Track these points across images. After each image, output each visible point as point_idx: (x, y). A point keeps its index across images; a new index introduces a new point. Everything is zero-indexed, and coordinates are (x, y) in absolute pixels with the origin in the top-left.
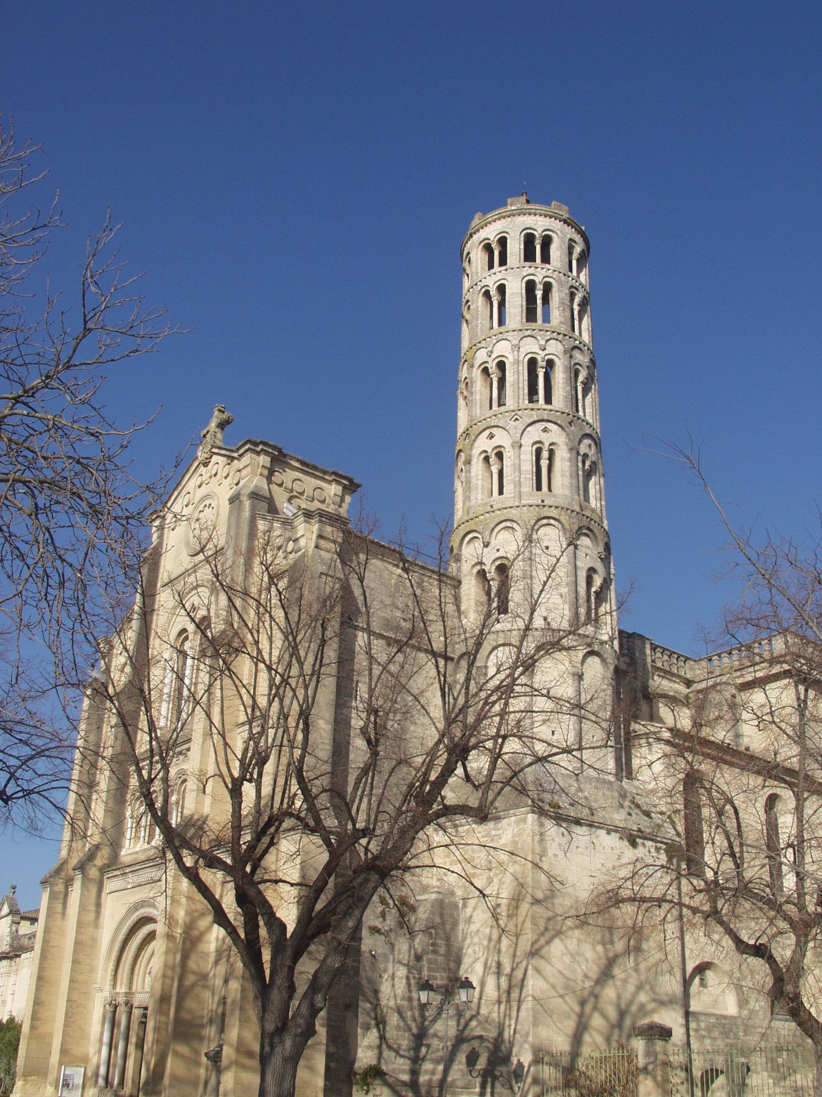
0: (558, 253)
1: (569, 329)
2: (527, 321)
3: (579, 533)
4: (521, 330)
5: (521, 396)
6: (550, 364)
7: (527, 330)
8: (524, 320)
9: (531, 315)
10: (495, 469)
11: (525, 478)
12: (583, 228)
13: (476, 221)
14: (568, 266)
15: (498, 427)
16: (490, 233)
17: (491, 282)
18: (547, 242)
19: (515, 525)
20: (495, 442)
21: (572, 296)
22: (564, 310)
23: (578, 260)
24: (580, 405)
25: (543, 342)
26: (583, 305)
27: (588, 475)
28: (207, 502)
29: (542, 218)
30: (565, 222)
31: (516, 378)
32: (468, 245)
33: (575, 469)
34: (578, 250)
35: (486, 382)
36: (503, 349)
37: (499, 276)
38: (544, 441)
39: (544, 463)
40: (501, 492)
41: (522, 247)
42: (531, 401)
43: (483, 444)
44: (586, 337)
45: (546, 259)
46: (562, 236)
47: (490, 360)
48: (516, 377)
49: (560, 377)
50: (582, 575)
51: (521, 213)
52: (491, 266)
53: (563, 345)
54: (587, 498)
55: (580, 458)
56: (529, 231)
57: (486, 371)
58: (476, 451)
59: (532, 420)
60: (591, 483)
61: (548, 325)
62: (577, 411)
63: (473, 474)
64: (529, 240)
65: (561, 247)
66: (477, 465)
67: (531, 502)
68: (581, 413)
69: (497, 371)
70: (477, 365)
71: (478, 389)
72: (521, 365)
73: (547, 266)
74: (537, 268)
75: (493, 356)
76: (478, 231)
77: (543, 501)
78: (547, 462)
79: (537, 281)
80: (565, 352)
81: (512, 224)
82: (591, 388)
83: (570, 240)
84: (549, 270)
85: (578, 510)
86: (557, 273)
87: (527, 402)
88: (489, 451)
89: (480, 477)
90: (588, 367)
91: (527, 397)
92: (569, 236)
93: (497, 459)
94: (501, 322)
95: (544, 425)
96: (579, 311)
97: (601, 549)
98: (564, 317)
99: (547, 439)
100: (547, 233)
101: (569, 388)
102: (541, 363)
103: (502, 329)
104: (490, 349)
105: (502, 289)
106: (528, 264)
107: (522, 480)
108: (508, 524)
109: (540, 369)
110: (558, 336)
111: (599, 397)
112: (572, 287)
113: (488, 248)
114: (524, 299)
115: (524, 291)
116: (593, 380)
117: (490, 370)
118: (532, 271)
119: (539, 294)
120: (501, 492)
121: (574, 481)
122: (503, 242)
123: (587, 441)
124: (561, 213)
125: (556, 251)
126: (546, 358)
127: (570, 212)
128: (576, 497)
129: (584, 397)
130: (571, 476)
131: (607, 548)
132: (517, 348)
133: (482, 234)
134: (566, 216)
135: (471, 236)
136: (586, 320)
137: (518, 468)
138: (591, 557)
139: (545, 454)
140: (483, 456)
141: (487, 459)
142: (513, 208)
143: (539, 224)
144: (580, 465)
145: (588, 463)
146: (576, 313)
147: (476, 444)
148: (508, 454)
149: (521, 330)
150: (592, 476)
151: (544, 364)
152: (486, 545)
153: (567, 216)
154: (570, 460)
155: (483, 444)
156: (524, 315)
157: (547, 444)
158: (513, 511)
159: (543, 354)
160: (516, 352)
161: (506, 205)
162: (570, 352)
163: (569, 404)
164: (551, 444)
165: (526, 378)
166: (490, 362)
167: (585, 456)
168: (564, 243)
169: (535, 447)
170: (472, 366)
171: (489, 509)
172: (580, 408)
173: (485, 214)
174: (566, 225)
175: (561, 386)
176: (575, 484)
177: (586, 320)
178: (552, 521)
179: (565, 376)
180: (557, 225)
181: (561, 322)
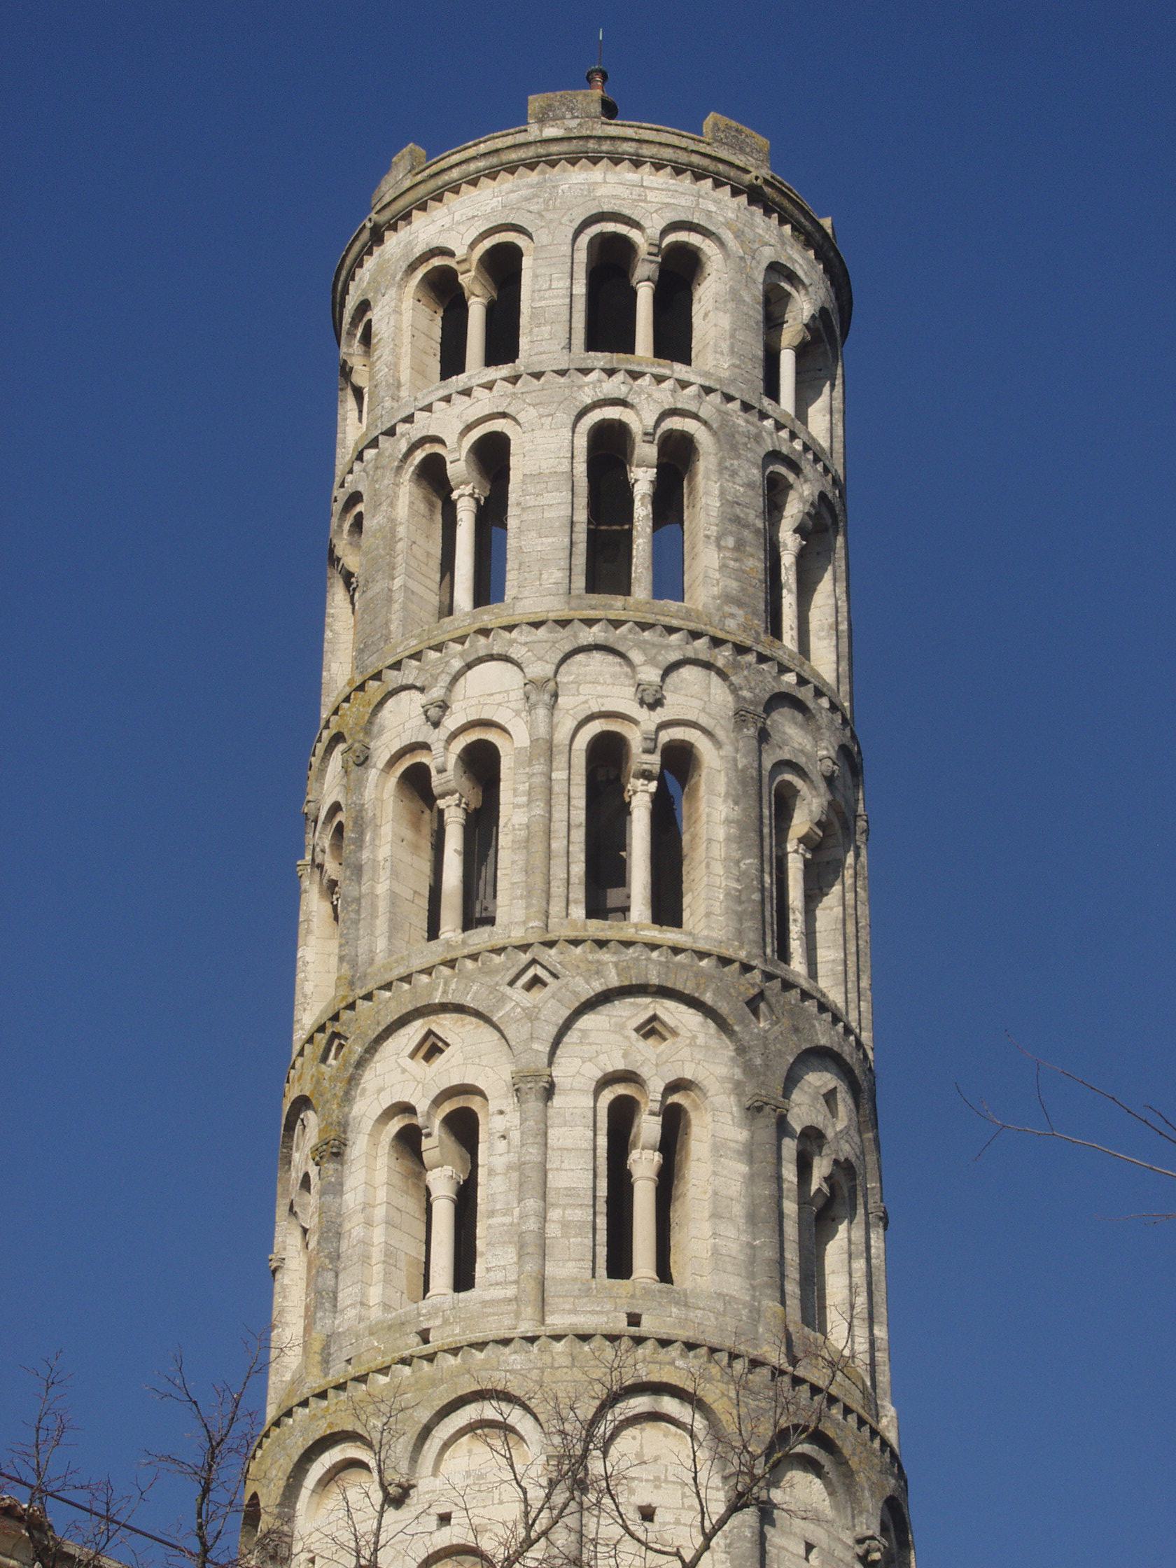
0: (725, 321)
1: (759, 624)
2: (591, 587)
3: (781, 1454)
4: (564, 623)
5: (558, 889)
6: (679, 763)
7: (590, 622)
8: (580, 582)
9: (605, 564)
10: (442, 1182)
11: (565, 1225)
12: (826, 223)
13: (398, 179)
14: (759, 373)
15: (460, 1009)
16: (455, 226)
17: (452, 424)
18: (680, 271)
19: (516, 1417)
20: (449, 1070)
21: (775, 492)
22: (740, 546)
23: (802, 351)
24: (796, 928)
25: (651, 675)
26: (819, 529)
27: (821, 1217)
29: (663, 178)
30: (755, 196)
31: (540, 814)
32: (365, 274)
33: (766, 1190)
34: (802, 308)
35: (416, 825)
36: (490, 693)
37: (483, 403)
38: (644, 1072)
39: (644, 1164)
40: (463, 1279)
41: (580, 289)
42: (596, 909)
43: (397, 1076)
44: (825, 660)
46: (739, 246)
47: (435, 738)
48: (539, 809)
49: (714, 816)
51: (582, 153)
52: (452, 362)
53: (734, 690)
54: (814, 1311)
55: (790, 1147)
56: (610, 227)
57: (417, 783)
58: (367, 1107)
59: (598, 986)
60: (835, 1251)
61: (672, 605)
62: (784, 954)
63: (352, 1199)
64: (609, 262)
65: (735, 296)
66: (371, 1168)
67: (586, 1322)
68: (798, 965)
69: (465, 784)
70: (381, 755)
71: (384, 851)
72: (560, 761)
73: (680, 370)
74: (635, 375)
75: (452, 722)
76: (406, 217)
77: (634, 1320)
78: (657, 1157)
79: (636, 427)
80: (741, 717)
81: (540, 198)
82: (840, 864)
83: (776, 268)
84: (684, 385)
85: (775, 1356)
86: (715, 398)
87: (578, 912)
88: (422, 1106)
89: (380, 1213)
90: (830, 780)
91: (579, 893)
92: (768, 254)
93: (451, 1144)
94: (487, 587)
95: (646, 1007)
96: (801, 557)
97: (869, 1524)
98: (739, 575)
99: (657, 1066)
100: (682, 236)
101: (750, 862)
102: (642, 758)
103: (490, 616)
104: (437, 693)
105: (492, 455)
106: (601, 359)
107: (553, 1230)
108: (489, 1410)
109: (640, 783)
110: (711, 649)
111: (871, 900)
112: (774, 456)
113: (443, 289)
114: (582, 500)
115: (581, 468)
116: (848, 831)
117: (436, 781)
118: (615, 386)
119: (642, 480)
120: (463, 1279)
121: (764, 1241)
122: (503, 265)
123: (819, 1080)
124: (740, 160)
125: (716, 313)
126: (665, 736)
127: (775, 159)
128: (770, 1304)
129: (812, 897)
130: (752, 1218)
131: (895, 1517)
132: (547, 692)
133: (425, 230)
134: (759, 171)
135: (377, 237)
136: (827, 595)
138: (828, 1556)
139: (648, 1127)
140: (396, 1125)
141: (410, 1141)
142: (550, 132)
143: (651, 201)
144: (790, 1173)
145: (821, 1168)
146: (788, 559)
147: (371, 1078)
148: (499, 1123)
149: (564, 623)
150: (835, 1221)
151: (654, 762)
153: (765, 172)
154: (749, 1153)
155: (397, 1076)
156: (580, 561)
157: (656, 1087)
158: (513, 1358)
159: (649, 720)
160: (541, 712)
161: (518, 119)
162: (757, 718)
163: (751, 925)
164: (677, 1086)
165: (580, 816)
166: (437, 747)
167: (812, 1138)
168: (750, 279)
169: (608, 1096)
170: (363, 761)
171: (412, 1345)
172: (796, 946)
173: (435, 149)
174: (758, 211)
175: (719, 851)
176: (770, 1253)
177: (827, 595)
178: (669, 1405)
179: (736, 813)
180: (720, 207)
181: (728, 598)
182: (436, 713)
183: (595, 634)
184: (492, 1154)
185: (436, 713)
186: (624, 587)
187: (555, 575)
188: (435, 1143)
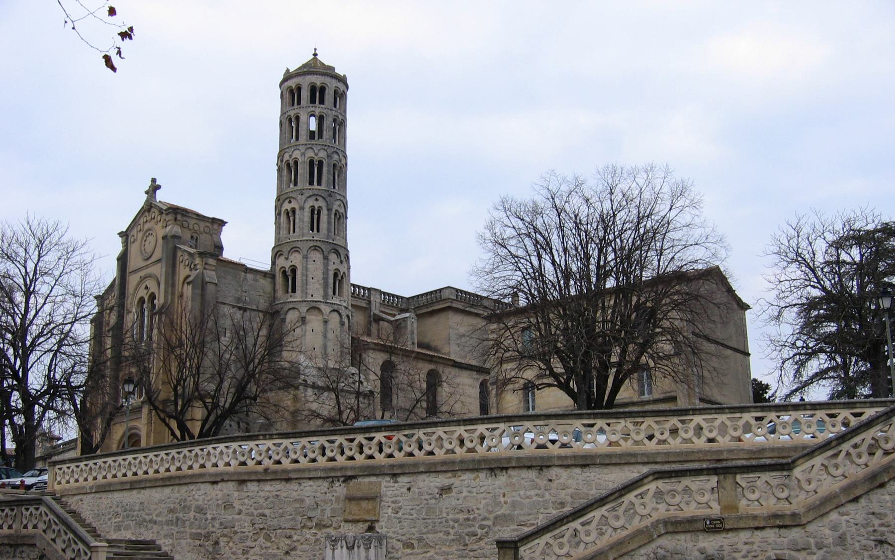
6: (321, 163)
18: (323, 90)
36: (297, 154)
39: (316, 217)
40: (294, 232)
45: (322, 102)
52: (293, 105)
58: (283, 209)
64: (313, 89)
105: (298, 118)
118: (313, 109)
120: (294, 232)
122: (299, 89)
132: (303, 154)
137: (302, 220)
141: (288, 213)
182: (291, 156)
184: (297, 217)
185: (291, 156)
187: (305, 137)
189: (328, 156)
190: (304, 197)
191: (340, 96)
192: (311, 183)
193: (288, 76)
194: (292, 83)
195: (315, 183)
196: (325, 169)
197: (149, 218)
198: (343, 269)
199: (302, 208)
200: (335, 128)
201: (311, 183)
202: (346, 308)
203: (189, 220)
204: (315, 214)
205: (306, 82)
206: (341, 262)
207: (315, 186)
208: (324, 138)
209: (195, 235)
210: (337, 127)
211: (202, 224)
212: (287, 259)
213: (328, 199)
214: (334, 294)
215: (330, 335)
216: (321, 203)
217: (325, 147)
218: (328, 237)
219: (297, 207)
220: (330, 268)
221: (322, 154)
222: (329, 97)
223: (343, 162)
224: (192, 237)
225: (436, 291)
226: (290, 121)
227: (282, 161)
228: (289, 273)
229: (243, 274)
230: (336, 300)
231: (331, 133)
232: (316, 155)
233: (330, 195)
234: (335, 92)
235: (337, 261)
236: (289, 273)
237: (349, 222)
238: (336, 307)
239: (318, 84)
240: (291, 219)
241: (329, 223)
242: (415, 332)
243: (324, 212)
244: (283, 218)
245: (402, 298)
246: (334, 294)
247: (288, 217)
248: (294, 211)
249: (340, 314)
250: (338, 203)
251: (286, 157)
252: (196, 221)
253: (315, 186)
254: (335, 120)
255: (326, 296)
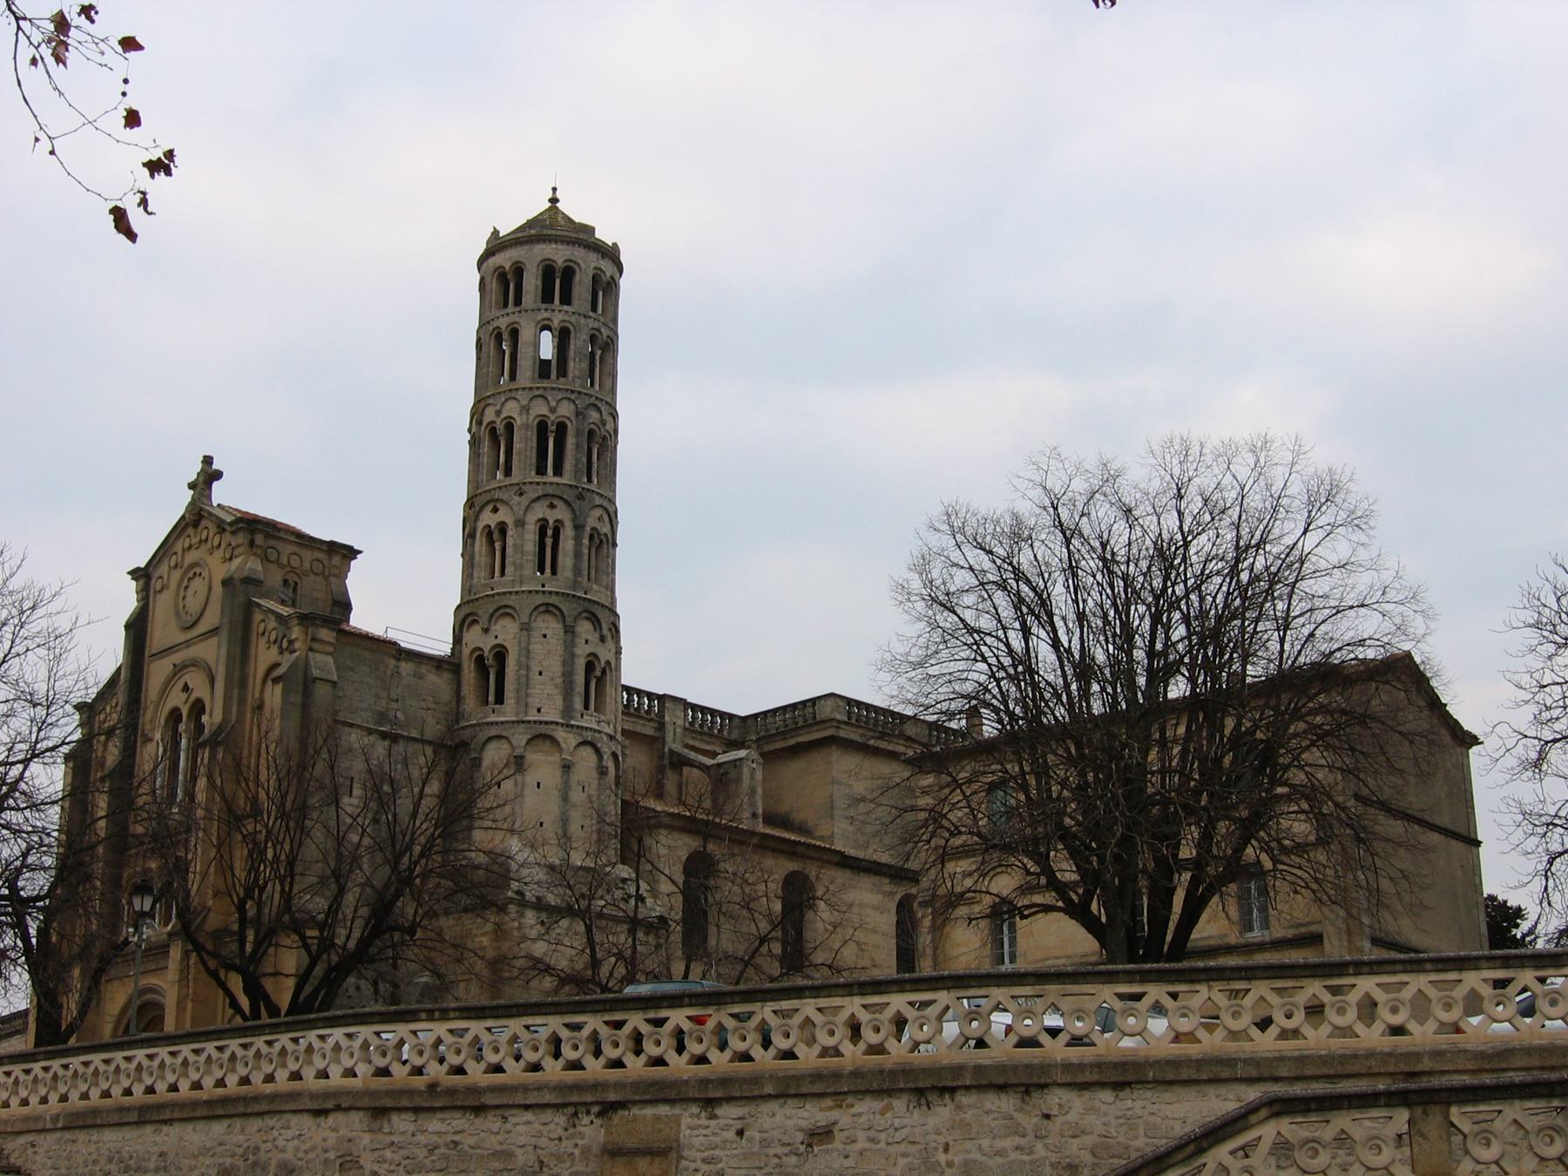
2: (541, 376)
6: (561, 429)
18: (569, 273)
28: (198, 570)
31: (524, 443)
36: (511, 409)
39: (549, 541)
40: (503, 573)
45: (566, 299)
50: (581, 663)
52: (506, 305)
58: (480, 525)
64: (548, 271)
99: (552, 517)
105: (514, 334)
106: (544, 306)
120: (503, 573)
122: (519, 271)
132: (525, 409)
137: (519, 548)
139: (550, 532)
141: (490, 534)
152: (486, 631)
182: (498, 413)
183: (537, 393)
184: (510, 541)
185: (498, 413)
186: (548, 377)
187: (529, 373)
188: (496, 536)
189: (578, 414)
190: (525, 501)
191: (606, 289)
192: (541, 470)
193: (496, 245)
194: (504, 259)
195: (550, 471)
196: (570, 441)
197: (195, 541)
198: (605, 654)
199: (520, 523)
200: (592, 354)
201: (541, 470)
202: (611, 737)
203: (280, 546)
204: (548, 535)
205: (531, 257)
206: (603, 639)
207: (550, 476)
208: (570, 376)
209: (292, 578)
210: (599, 352)
211: (309, 556)
212: (486, 631)
213: (577, 504)
214: (586, 707)
215: (577, 796)
216: (562, 513)
217: (571, 395)
218: (575, 584)
219: (510, 521)
220: (578, 651)
221: (566, 410)
222: (581, 289)
223: (609, 427)
224: (285, 582)
225: (804, 703)
226: (499, 338)
227: (480, 423)
228: (490, 661)
229: (392, 662)
230: (589, 721)
231: (585, 365)
232: (553, 410)
233: (581, 497)
234: (596, 279)
235: (594, 637)
236: (490, 661)
237: (621, 554)
238: (589, 736)
239: (560, 262)
240: (498, 545)
241: (577, 555)
242: (759, 790)
243: (568, 533)
244: (480, 544)
245: (731, 716)
246: (586, 707)
247: (491, 542)
248: (502, 528)
249: (598, 751)
250: (597, 512)
251: (489, 415)
252: (296, 549)
253: (550, 476)
254: (593, 339)
255: (567, 711)
